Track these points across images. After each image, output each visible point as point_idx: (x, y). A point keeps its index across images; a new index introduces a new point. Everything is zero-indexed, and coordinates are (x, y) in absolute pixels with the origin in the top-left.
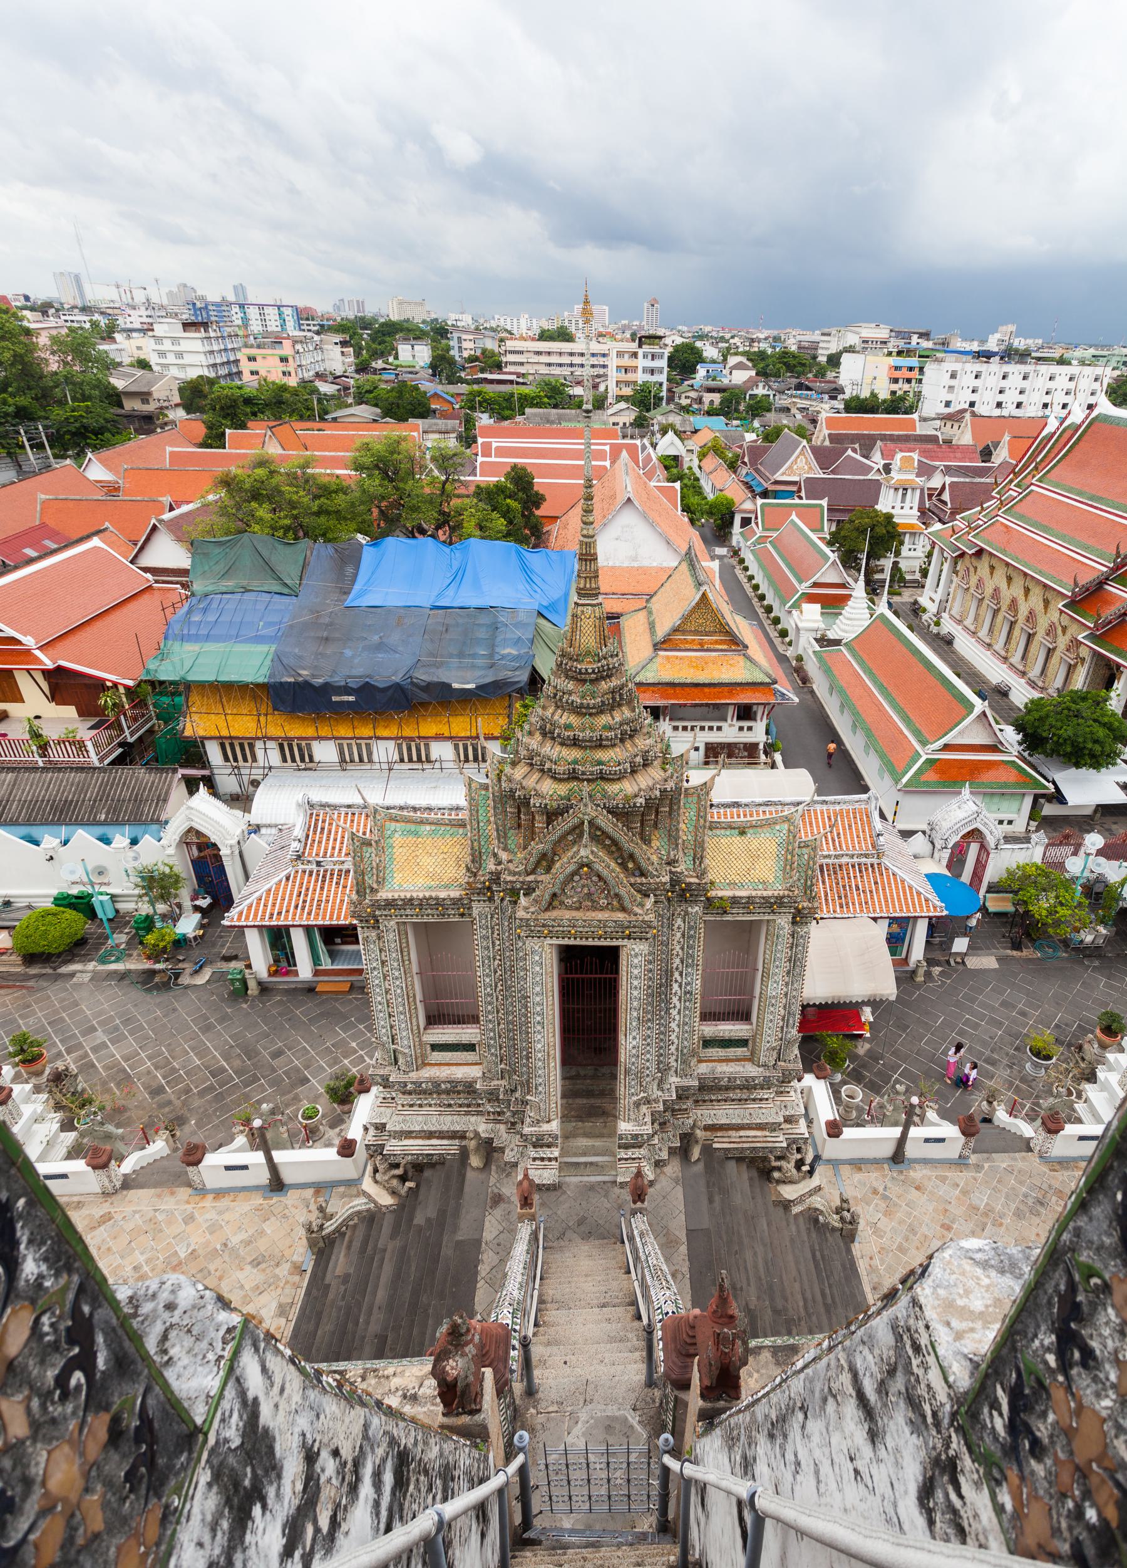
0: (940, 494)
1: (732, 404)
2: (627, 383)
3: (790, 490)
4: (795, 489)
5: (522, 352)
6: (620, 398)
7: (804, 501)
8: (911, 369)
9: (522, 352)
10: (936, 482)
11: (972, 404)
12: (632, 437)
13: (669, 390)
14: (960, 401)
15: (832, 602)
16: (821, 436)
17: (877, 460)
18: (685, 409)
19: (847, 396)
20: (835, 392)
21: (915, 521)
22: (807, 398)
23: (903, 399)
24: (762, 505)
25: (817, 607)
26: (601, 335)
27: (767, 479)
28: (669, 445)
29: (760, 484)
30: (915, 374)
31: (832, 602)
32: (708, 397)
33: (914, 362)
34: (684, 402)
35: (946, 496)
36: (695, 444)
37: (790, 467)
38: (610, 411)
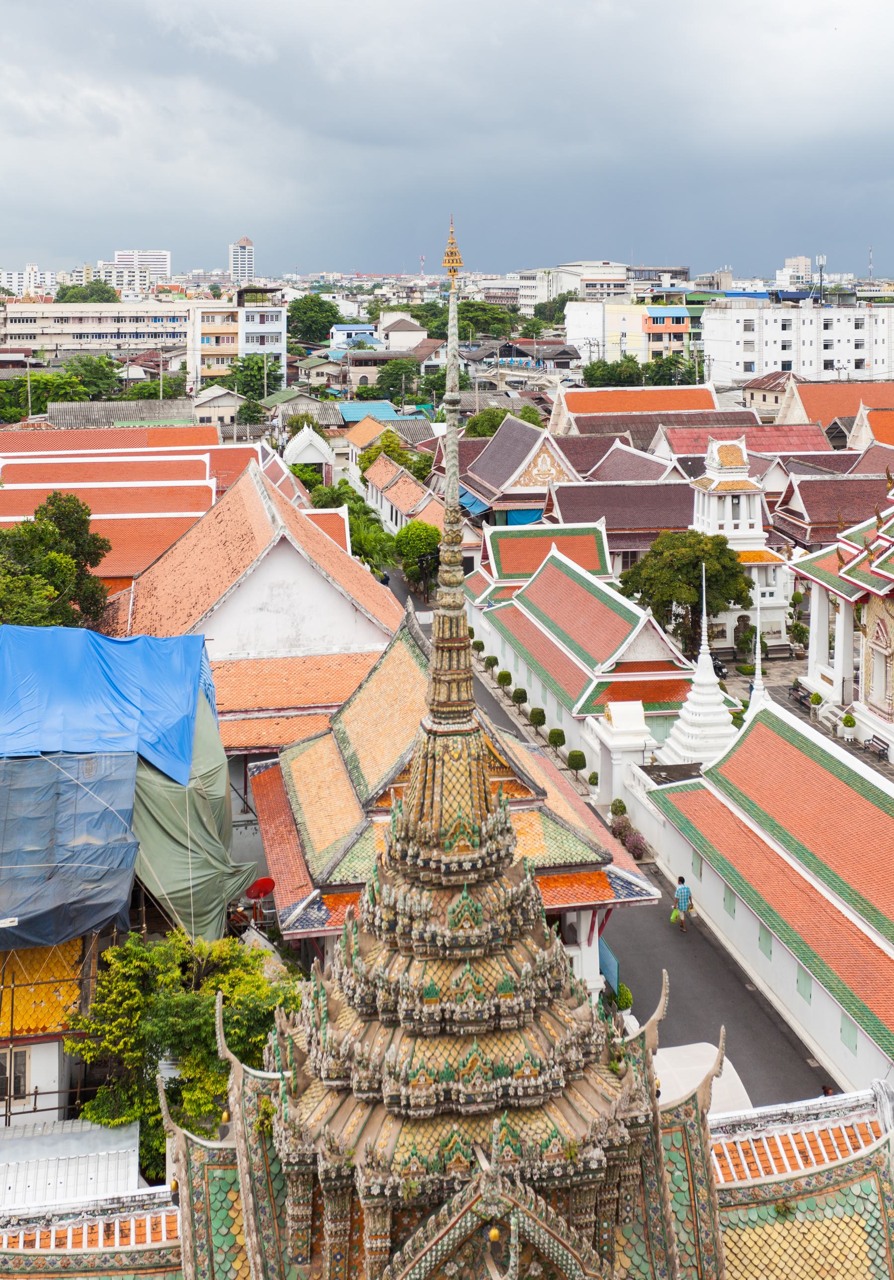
0: (786, 502)
1: (396, 381)
2: (220, 358)
3: (535, 507)
4: (542, 505)
5: (33, 320)
6: (208, 381)
7: (562, 526)
8: (678, 320)
9: (33, 320)
10: (776, 482)
11: (787, 366)
12: (240, 439)
13: (290, 365)
14: (768, 362)
15: (661, 697)
16: (563, 421)
17: (663, 453)
18: (320, 393)
19: (585, 362)
20: (564, 357)
21: (762, 547)
22: (525, 367)
23: (674, 362)
24: (494, 536)
25: (636, 708)
26: (162, 290)
27: (489, 494)
28: (306, 447)
29: (476, 501)
30: (686, 327)
31: (661, 697)
32: (356, 374)
33: (681, 310)
34: (316, 381)
35: (797, 503)
36: (351, 444)
37: (527, 472)
38: (197, 401)
